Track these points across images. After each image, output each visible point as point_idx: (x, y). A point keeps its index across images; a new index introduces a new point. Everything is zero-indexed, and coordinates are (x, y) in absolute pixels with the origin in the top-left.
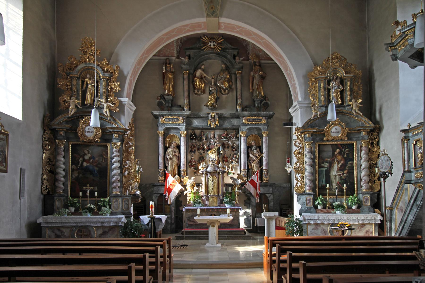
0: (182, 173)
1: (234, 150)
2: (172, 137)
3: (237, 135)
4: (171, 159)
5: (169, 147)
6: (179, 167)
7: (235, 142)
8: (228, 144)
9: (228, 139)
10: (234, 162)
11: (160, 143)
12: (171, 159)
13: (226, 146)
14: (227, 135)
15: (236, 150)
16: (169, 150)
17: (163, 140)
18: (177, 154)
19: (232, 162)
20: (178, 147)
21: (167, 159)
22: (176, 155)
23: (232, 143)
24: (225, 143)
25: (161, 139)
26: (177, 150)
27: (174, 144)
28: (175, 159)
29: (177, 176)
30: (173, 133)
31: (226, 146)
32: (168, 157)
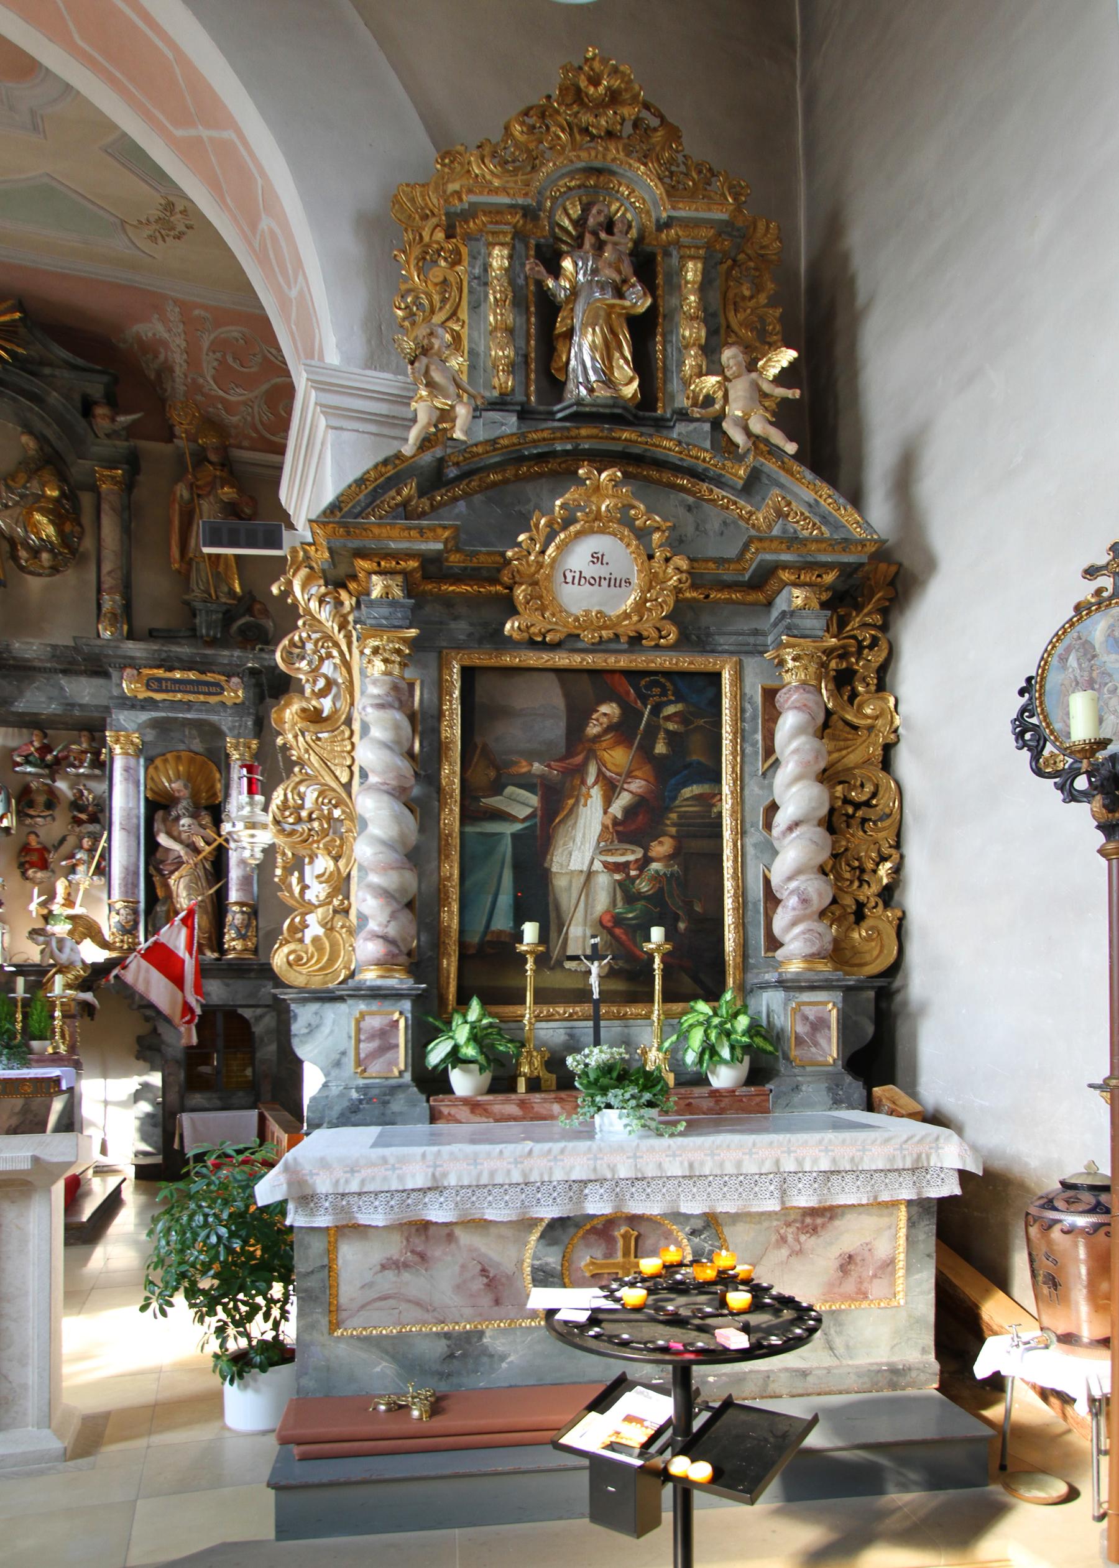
1: (84, 816)
3: (97, 753)
7: (92, 784)
9: (55, 768)
10: (81, 868)
14: (45, 749)
19: (73, 869)
23: (71, 788)
24: (34, 785)
31: (41, 799)
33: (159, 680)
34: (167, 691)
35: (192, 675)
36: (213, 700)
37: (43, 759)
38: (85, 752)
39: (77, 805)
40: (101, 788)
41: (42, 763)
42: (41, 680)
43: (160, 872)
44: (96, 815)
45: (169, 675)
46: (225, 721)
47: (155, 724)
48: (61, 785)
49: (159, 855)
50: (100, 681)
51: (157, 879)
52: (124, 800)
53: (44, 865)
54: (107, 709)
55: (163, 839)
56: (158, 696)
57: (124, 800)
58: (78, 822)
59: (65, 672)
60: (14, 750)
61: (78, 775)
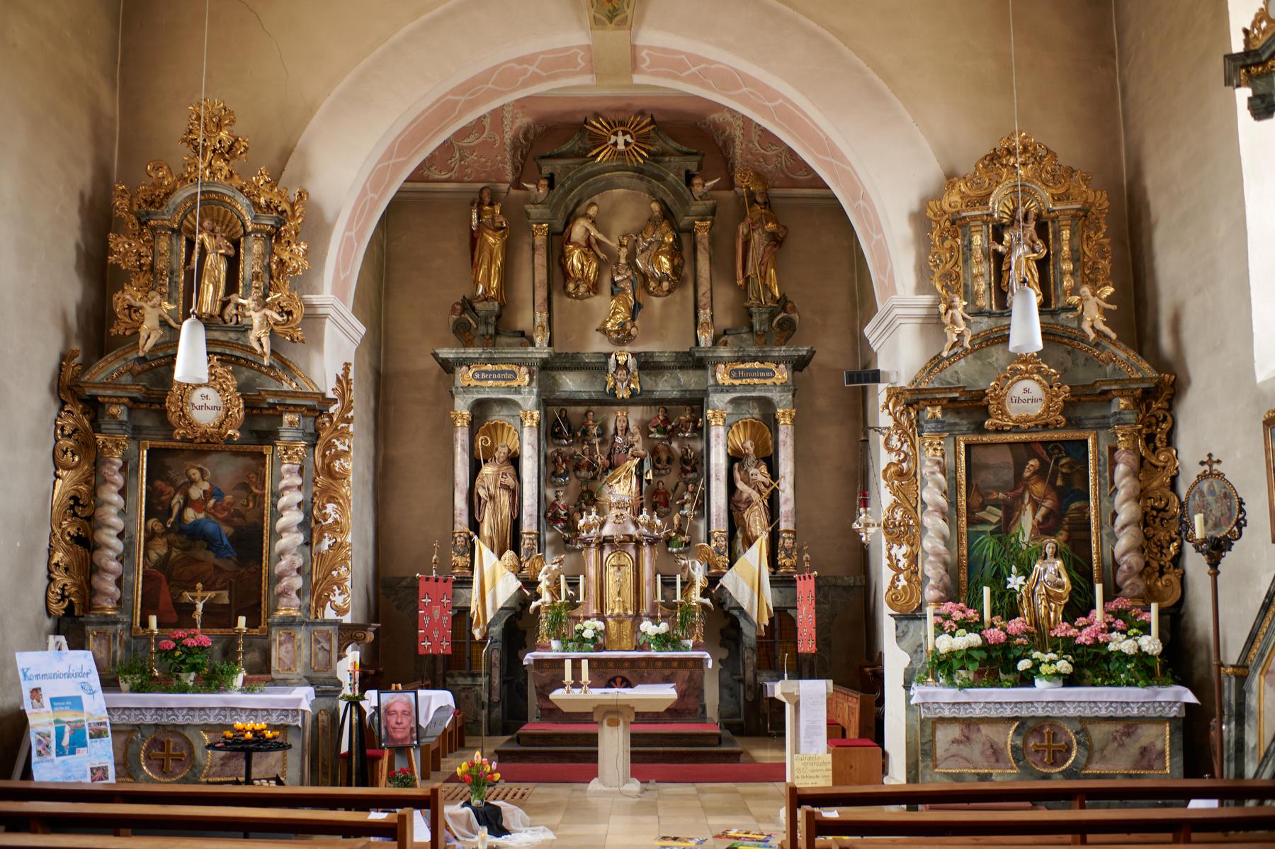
0: (526, 543)
1: (689, 468)
2: (494, 430)
3: (696, 422)
4: (492, 498)
5: (486, 462)
6: (516, 523)
7: (692, 443)
8: (669, 450)
9: (671, 434)
10: (687, 506)
11: (459, 450)
12: (492, 498)
13: (664, 457)
14: (667, 421)
15: (694, 470)
16: (488, 470)
17: (466, 438)
18: (510, 481)
19: (682, 506)
20: (514, 460)
21: (480, 498)
22: (506, 487)
25: (462, 437)
26: (511, 470)
27: (501, 453)
28: (504, 499)
29: (509, 554)
30: (498, 416)
31: (664, 457)
32: (482, 493)
33: (737, 370)
34: (741, 378)
35: (757, 365)
36: (769, 382)
37: (665, 428)
38: (688, 421)
39: (684, 460)
40: (699, 445)
41: (664, 431)
42: (667, 375)
43: (738, 508)
44: (696, 465)
45: (742, 366)
46: (775, 396)
47: (734, 401)
48: (675, 445)
49: (736, 497)
50: (700, 372)
51: (735, 514)
52: (718, 460)
53: (666, 504)
54: (705, 393)
55: (740, 485)
56: (737, 382)
57: (718, 460)
58: (686, 472)
59: (681, 368)
60: (648, 422)
61: (684, 437)
